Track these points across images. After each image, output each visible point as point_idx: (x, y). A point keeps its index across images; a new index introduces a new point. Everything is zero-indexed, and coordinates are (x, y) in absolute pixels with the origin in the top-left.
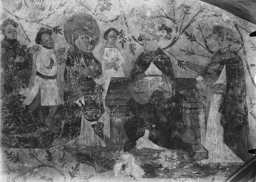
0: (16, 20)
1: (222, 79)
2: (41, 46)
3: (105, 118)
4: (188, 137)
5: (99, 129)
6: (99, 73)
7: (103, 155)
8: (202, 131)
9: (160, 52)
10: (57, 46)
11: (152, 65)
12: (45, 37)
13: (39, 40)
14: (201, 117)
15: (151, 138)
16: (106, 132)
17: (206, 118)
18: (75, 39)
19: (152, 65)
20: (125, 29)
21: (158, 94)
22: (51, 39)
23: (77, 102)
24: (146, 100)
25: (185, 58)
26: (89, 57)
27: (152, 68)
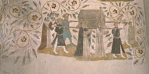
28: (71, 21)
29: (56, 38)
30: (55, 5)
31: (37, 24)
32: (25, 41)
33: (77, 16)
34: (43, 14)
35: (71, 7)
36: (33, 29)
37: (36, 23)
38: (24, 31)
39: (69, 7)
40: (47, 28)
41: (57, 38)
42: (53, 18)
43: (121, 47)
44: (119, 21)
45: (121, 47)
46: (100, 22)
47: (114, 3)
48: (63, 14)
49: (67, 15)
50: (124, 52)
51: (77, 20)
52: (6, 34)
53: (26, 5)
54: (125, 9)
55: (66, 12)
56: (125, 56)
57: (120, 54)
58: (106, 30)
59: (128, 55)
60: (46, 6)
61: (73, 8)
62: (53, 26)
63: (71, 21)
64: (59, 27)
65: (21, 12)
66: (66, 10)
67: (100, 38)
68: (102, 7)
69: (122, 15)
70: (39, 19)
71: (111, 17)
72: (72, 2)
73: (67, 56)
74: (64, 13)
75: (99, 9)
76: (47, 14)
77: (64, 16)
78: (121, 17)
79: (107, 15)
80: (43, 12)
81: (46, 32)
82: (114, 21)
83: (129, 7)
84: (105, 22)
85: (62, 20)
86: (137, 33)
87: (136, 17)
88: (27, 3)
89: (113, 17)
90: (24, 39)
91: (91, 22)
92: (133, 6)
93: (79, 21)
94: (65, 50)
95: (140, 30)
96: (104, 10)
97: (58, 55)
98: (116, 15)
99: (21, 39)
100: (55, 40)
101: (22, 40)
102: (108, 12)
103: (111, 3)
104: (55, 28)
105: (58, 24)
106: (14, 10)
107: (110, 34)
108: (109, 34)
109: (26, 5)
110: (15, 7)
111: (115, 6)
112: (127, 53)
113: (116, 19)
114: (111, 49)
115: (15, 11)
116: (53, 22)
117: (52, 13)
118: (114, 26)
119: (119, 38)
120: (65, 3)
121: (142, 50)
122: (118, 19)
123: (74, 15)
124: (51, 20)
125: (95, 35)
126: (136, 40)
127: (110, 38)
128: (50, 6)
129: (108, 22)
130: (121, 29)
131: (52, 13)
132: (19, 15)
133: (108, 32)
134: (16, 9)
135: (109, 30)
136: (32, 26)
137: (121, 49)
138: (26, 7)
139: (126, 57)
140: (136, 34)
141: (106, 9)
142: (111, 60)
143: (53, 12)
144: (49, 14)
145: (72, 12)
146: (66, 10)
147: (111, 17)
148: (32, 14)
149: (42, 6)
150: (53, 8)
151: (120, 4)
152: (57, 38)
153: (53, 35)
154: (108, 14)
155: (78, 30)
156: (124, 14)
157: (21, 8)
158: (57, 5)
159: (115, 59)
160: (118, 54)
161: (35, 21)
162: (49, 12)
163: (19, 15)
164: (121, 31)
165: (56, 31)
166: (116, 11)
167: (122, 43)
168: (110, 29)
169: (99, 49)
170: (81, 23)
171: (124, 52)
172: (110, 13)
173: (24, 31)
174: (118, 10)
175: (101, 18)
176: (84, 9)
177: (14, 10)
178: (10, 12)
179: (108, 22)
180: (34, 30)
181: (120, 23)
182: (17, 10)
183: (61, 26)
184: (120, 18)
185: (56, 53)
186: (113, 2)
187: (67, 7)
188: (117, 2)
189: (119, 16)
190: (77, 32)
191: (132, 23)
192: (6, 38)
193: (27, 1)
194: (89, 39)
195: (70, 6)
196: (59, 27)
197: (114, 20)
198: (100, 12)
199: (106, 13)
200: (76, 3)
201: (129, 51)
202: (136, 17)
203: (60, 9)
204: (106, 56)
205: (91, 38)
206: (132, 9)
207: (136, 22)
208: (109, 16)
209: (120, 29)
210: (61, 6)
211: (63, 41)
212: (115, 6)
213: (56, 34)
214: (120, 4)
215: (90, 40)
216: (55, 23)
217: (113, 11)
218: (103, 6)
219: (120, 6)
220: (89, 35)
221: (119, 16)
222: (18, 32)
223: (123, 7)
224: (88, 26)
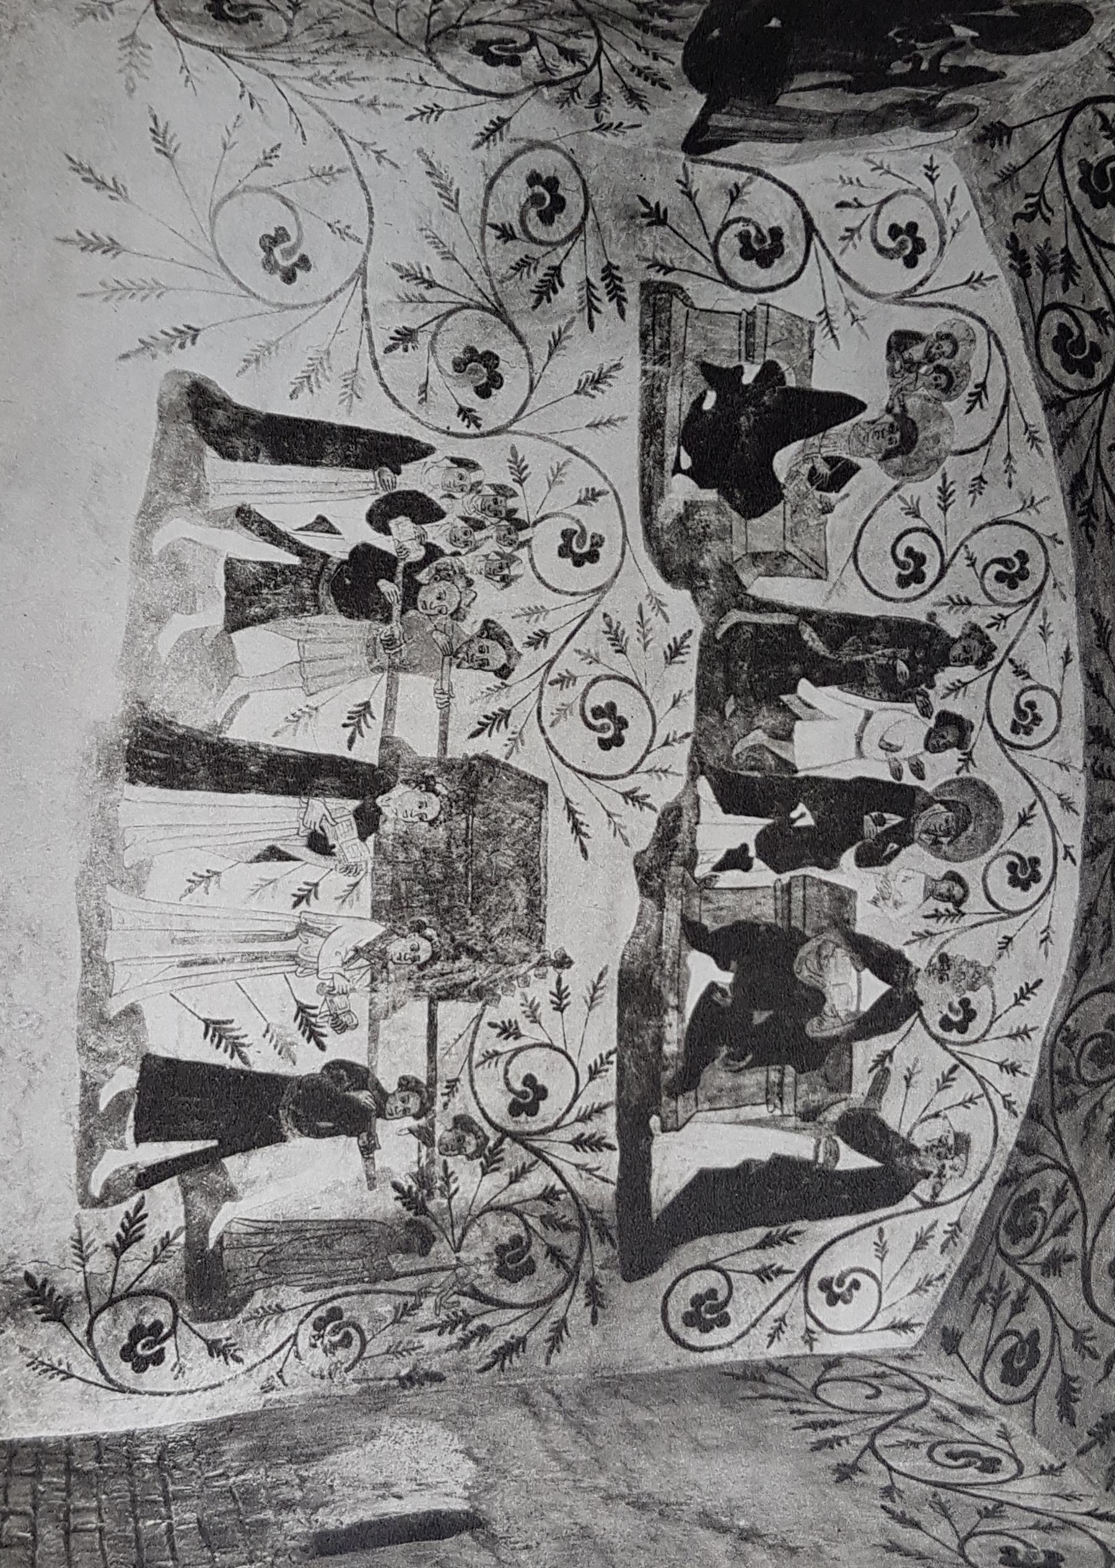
0: (992, 664)
1: (851, 1160)
2: (932, 723)
3: (762, 875)
4: (716, 1076)
5: (736, 860)
6: (865, 860)
7: (676, 870)
8: (728, 1114)
9: (914, 1004)
10: (927, 758)
11: (885, 987)
12: (951, 735)
13: (947, 719)
14: (763, 1111)
15: (713, 987)
16: (731, 878)
17: (758, 1122)
18: (942, 802)
19: (885, 987)
20: (968, 921)
21: (816, 999)
22: (947, 746)
23: (802, 808)
24: (804, 975)
25: (897, 1067)
26: (903, 836)
27: (874, 988)
28: (446, 699)
29: (302, 551)
30: (592, 556)
31: (424, 388)
32: (269, 265)
33: (494, 745)
34: (514, 454)
35: (572, 694)
36: (379, 352)
37: (435, 379)
38: (362, 271)
39: (563, 681)
40: (388, 474)
41: (296, 560)
42: (478, 535)
43: (198, 1146)
44: (439, 1132)
45: (198, 1146)
46: (435, 957)
47: (605, 1090)
48: (506, 624)
49: (498, 657)
50: (150, 1177)
51: (462, 747)
52: (347, 92)
53: (591, 306)
54: (549, 1195)
55: (528, 653)
56: (110, 1195)
57: (129, 1136)
58: (359, 1005)
59: (113, 1218)
60: (580, 477)
61: (563, 710)
62: (403, 527)
63: (446, 699)
64: (400, 578)
65: (537, 251)
66: (545, 653)
67: (291, 946)
68: (565, 974)
69: (490, 1161)
70: (465, 413)
71: (477, 1057)
72: (612, 707)
73: (130, 642)
74: (518, 632)
75: (551, 947)
76: (508, 480)
77: (489, 630)
78: (478, 1153)
79: (492, 1014)
80: (526, 448)
81: (346, 461)
82: (441, 1088)
83: (566, 1228)
84: (432, 1001)
85: (457, 614)
86: (321, 1312)
87: (475, 1294)
88: (609, 307)
89: (478, 1073)
90: (288, 253)
91: (437, 872)
92: (573, 1276)
93: (448, 767)
94: (179, 624)
95: (356, 1342)
96: (541, 991)
97: (143, 559)
98: (497, 1103)
99: (293, 233)
100: (273, 535)
101: (275, 241)
102: (525, 1026)
103: (604, 1060)
104: (383, 543)
105: (422, 577)
106: (552, 184)
107: (322, 1047)
108: (327, 1030)
109: (591, 306)
110: (574, 200)
111: (576, 1096)
112: (139, 1207)
113: (457, 1107)
114: (187, 1054)
115: (536, 199)
116: (435, 533)
117: (521, 525)
118: (390, 1084)
119: (287, 1125)
120: (605, 648)
121: (158, 1359)
122: (462, 1123)
123: (503, 716)
124: (456, 509)
125: (315, 906)
126: (259, 1299)
127: (284, 1050)
128: (579, 512)
129: (432, 1025)
130: (368, 1150)
131: (521, 525)
132: (506, 234)
133: (340, 1027)
134: (559, 204)
135: (363, 1032)
136: (406, 336)
137: (177, 1149)
138: (569, 295)
139: (100, 1203)
140: (319, 1295)
141: (546, 1011)
142: (82, 1045)
143: (523, 535)
144: (511, 503)
145: (531, 703)
146: (545, 653)
147: (477, 1057)
148: (508, 352)
149: (585, 441)
150: (567, 535)
151: (595, 1144)
152: (296, 560)
153: (322, 525)
154: (508, 1030)
155: (367, 752)
156: (500, 1178)
157: (561, 251)
158: (593, 574)
159: (90, 1089)
160: (131, 1115)
161: (449, 369)
162: (525, 505)
163: (506, 234)
164: (346, 1147)
165: (363, 554)
166: (533, 1110)
167: (232, 1163)
168: (374, 1039)
169: (184, 941)
170: (426, 784)
171: (150, 1177)
172: (512, 1044)
173: (362, 271)
174: (533, 1124)
175: (465, 960)
176: (555, 820)
177: (552, 184)
178: (533, 145)
179: (432, 1025)
180: (366, 359)
181: (425, 1136)
182: (547, 218)
183: (410, 598)
184: (471, 1147)
185: (160, 541)
186: (613, 1069)
187: (568, 662)
188: (611, 1115)
189: (489, 1131)
190: (351, 741)
191: (421, 1263)
192: (308, 88)
193: (622, 313)
194: (279, 845)
195: (581, 685)
196: (400, 578)
197: (452, 1085)
198: (524, 958)
199: (509, 1008)
200: (605, 745)
201: (153, 1233)
202: (475, 1294)
203: (549, 599)
204: (114, 1007)
205: (299, 863)
206: (544, 1265)
207: (429, 1302)
208: (488, 1040)
209: (371, 1135)
210: (586, 606)
211: (272, 616)
212: (576, 1096)
213: (338, 549)
214: (595, 1144)
215: (274, 854)
216: (433, 552)
217: (529, 1080)
218: (576, 981)
219: (579, 1143)
220: (319, 843)
221: (489, 1131)
222: (352, 210)
223: (570, 1173)
224: (405, 842)
